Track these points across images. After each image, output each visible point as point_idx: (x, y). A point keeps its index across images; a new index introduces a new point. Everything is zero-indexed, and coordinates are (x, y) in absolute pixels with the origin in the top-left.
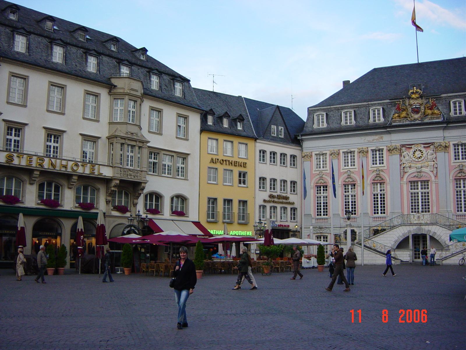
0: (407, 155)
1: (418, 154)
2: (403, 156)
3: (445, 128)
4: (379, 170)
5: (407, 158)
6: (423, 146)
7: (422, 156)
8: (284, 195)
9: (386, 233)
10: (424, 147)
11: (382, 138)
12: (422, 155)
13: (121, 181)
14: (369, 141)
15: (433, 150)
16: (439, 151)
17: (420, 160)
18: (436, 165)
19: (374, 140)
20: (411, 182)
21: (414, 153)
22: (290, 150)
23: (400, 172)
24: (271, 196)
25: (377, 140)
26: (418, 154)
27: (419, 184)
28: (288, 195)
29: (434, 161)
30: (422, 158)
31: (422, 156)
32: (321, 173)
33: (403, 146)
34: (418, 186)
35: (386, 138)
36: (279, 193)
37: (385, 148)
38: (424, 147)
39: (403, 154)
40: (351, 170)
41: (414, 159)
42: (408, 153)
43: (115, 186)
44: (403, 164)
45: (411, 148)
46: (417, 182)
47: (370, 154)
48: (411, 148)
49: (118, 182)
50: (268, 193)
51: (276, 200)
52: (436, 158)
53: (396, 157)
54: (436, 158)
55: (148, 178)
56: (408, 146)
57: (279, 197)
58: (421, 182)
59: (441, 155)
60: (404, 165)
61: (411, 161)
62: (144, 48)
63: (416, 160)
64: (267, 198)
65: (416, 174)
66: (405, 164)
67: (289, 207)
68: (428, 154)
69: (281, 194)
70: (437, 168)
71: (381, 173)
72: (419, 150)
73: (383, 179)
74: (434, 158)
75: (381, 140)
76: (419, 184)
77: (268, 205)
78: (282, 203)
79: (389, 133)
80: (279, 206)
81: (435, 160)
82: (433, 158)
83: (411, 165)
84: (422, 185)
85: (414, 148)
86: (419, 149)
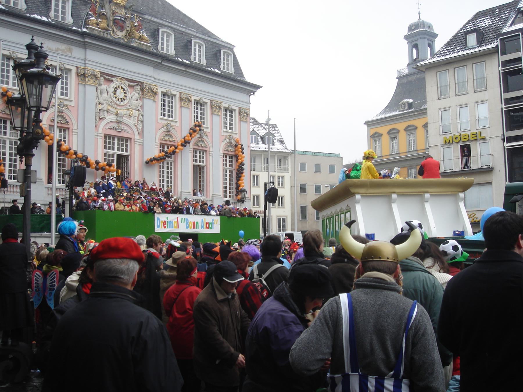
0: (106, 90)
1: (120, 94)
5: (105, 95)
6: (127, 83)
10: (130, 86)
11: (70, 50)
14: (50, 50)
17: (122, 103)
19: (58, 50)
20: (106, 136)
21: (115, 91)
25: (63, 51)
26: (120, 94)
29: (138, 110)
30: (126, 102)
35: (78, 53)
41: (114, 99)
42: (108, 89)
45: (112, 81)
46: (113, 137)
56: (108, 78)
63: (118, 102)
65: (114, 125)
66: (102, 104)
70: (142, 121)
71: (65, 111)
73: (67, 122)
75: (70, 55)
81: (140, 109)
85: (116, 83)
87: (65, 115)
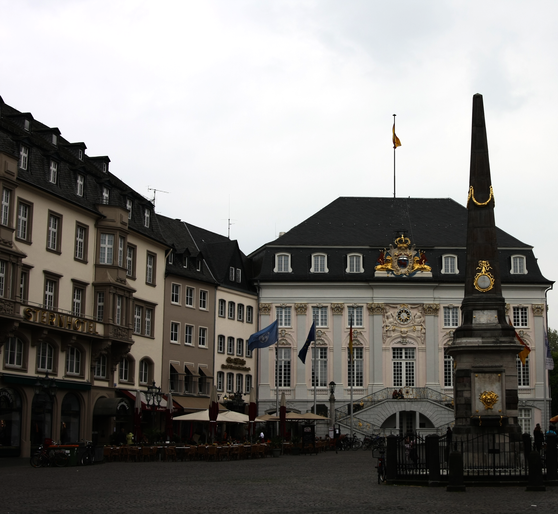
0: (391, 316)
1: (404, 316)
2: (386, 317)
3: (435, 288)
4: (357, 333)
5: (391, 320)
6: (409, 306)
7: (408, 318)
8: (241, 358)
9: (369, 410)
10: (411, 308)
12: (409, 317)
13: (114, 342)
15: (421, 313)
16: (428, 314)
17: (406, 323)
18: (423, 331)
20: (394, 349)
22: (247, 301)
23: (383, 336)
24: (229, 360)
26: (404, 316)
27: (404, 352)
28: (244, 358)
29: (421, 325)
30: (409, 321)
31: (408, 318)
32: (283, 331)
33: (387, 304)
34: (401, 353)
36: (235, 357)
37: (365, 306)
38: (411, 308)
39: (386, 315)
40: (321, 330)
41: (399, 321)
43: (105, 349)
44: (386, 326)
46: (401, 349)
47: (346, 312)
48: (397, 307)
49: (110, 343)
50: (226, 356)
51: (233, 365)
52: (424, 322)
53: (378, 318)
54: (424, 322)
55: (134, 338)
57: (236, 361)
58: (406, 349)
59: (429, 319)
60: (388, 328)
61: (396, 324)
62: (107, 157)
63: (402, 323)
64: (225, 364)
65: (399, 340)
66: (389, 326)
67: (244, 374)
68: (416, 316)
69: (238, 357)
70: (424, 333)
72: (405, 311)
74: (422, 321)
76: (404, 352)
77: (226, 372)
78: (238, 369)
79: (372, 288)
80: (235, 373)
81: (423, 324)
82: (421, 322)
83: (396, 329)
84: (406, 353)
86: (406, 310)
87: (359, 339)
